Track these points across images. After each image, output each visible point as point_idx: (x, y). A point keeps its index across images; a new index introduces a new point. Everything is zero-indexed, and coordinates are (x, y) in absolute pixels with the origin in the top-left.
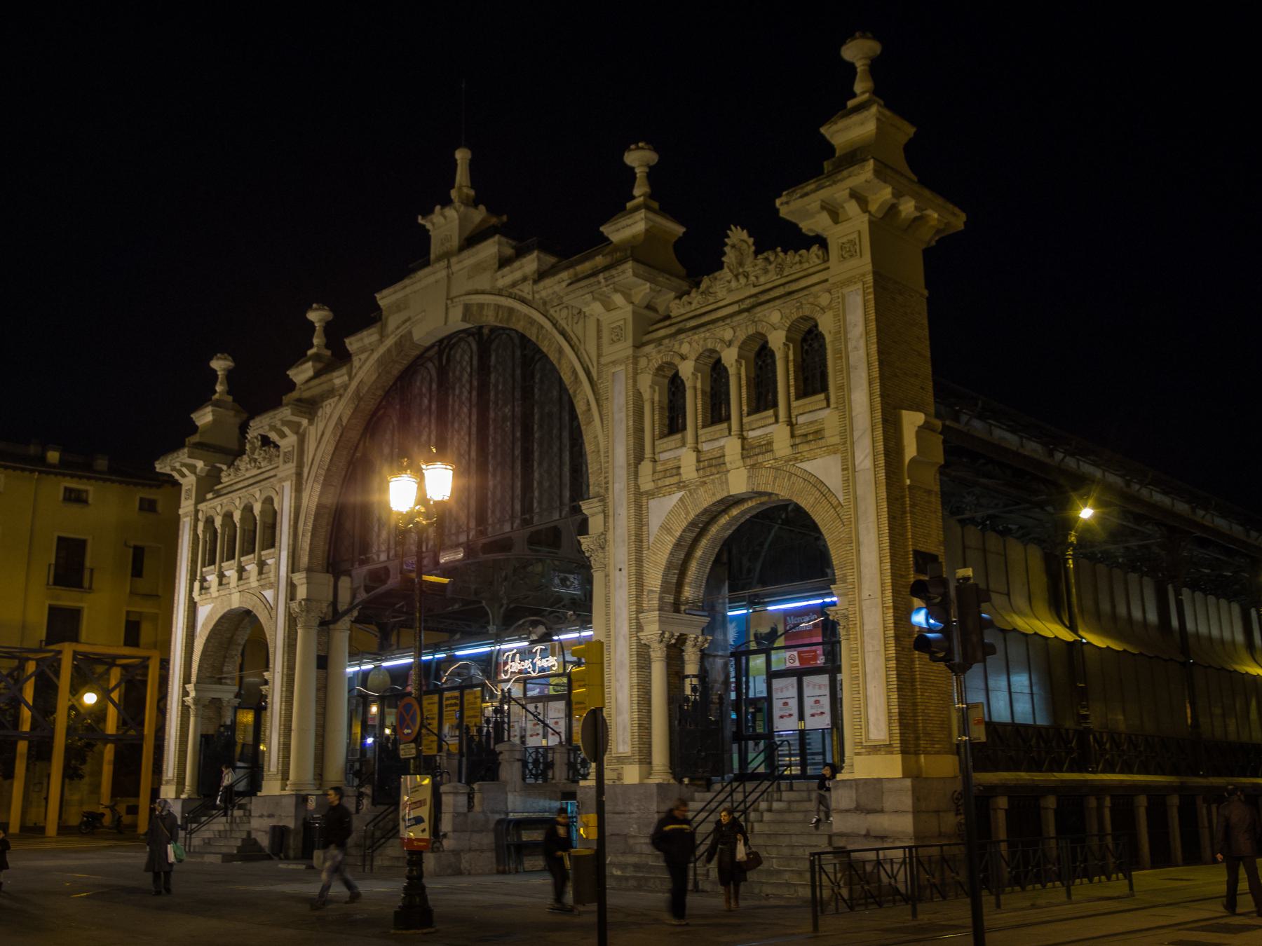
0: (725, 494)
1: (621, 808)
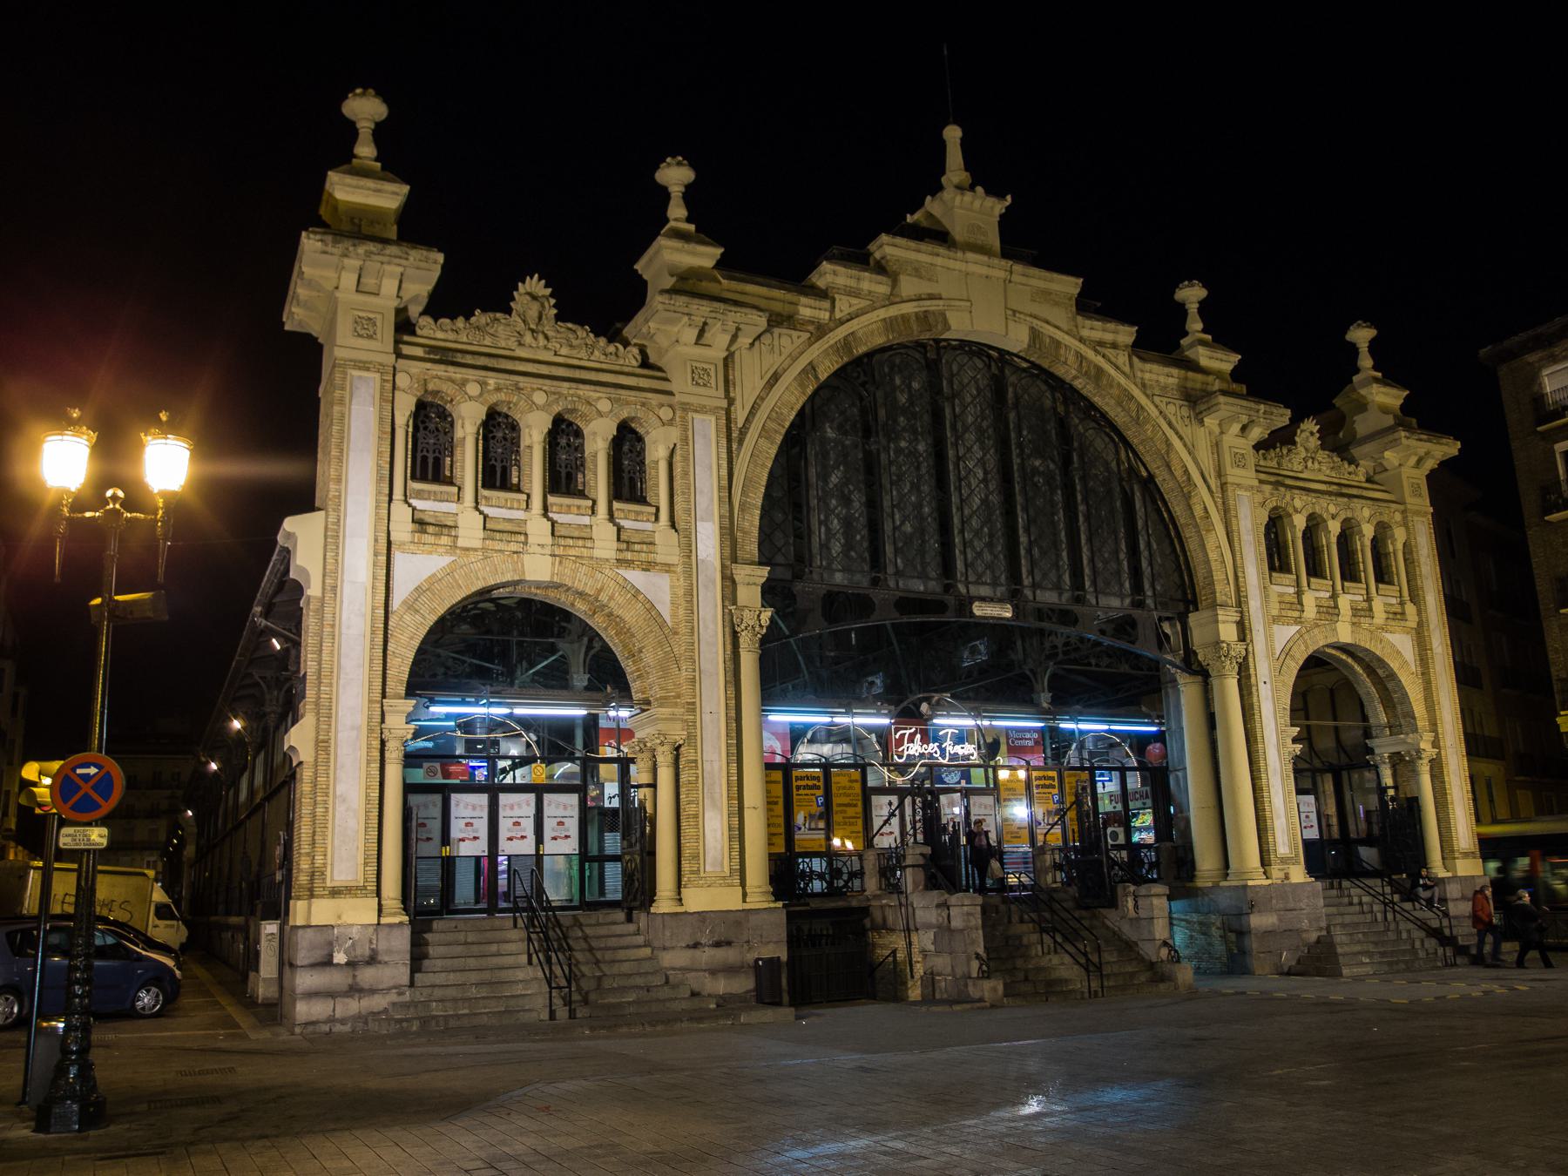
1: (1291, 905)
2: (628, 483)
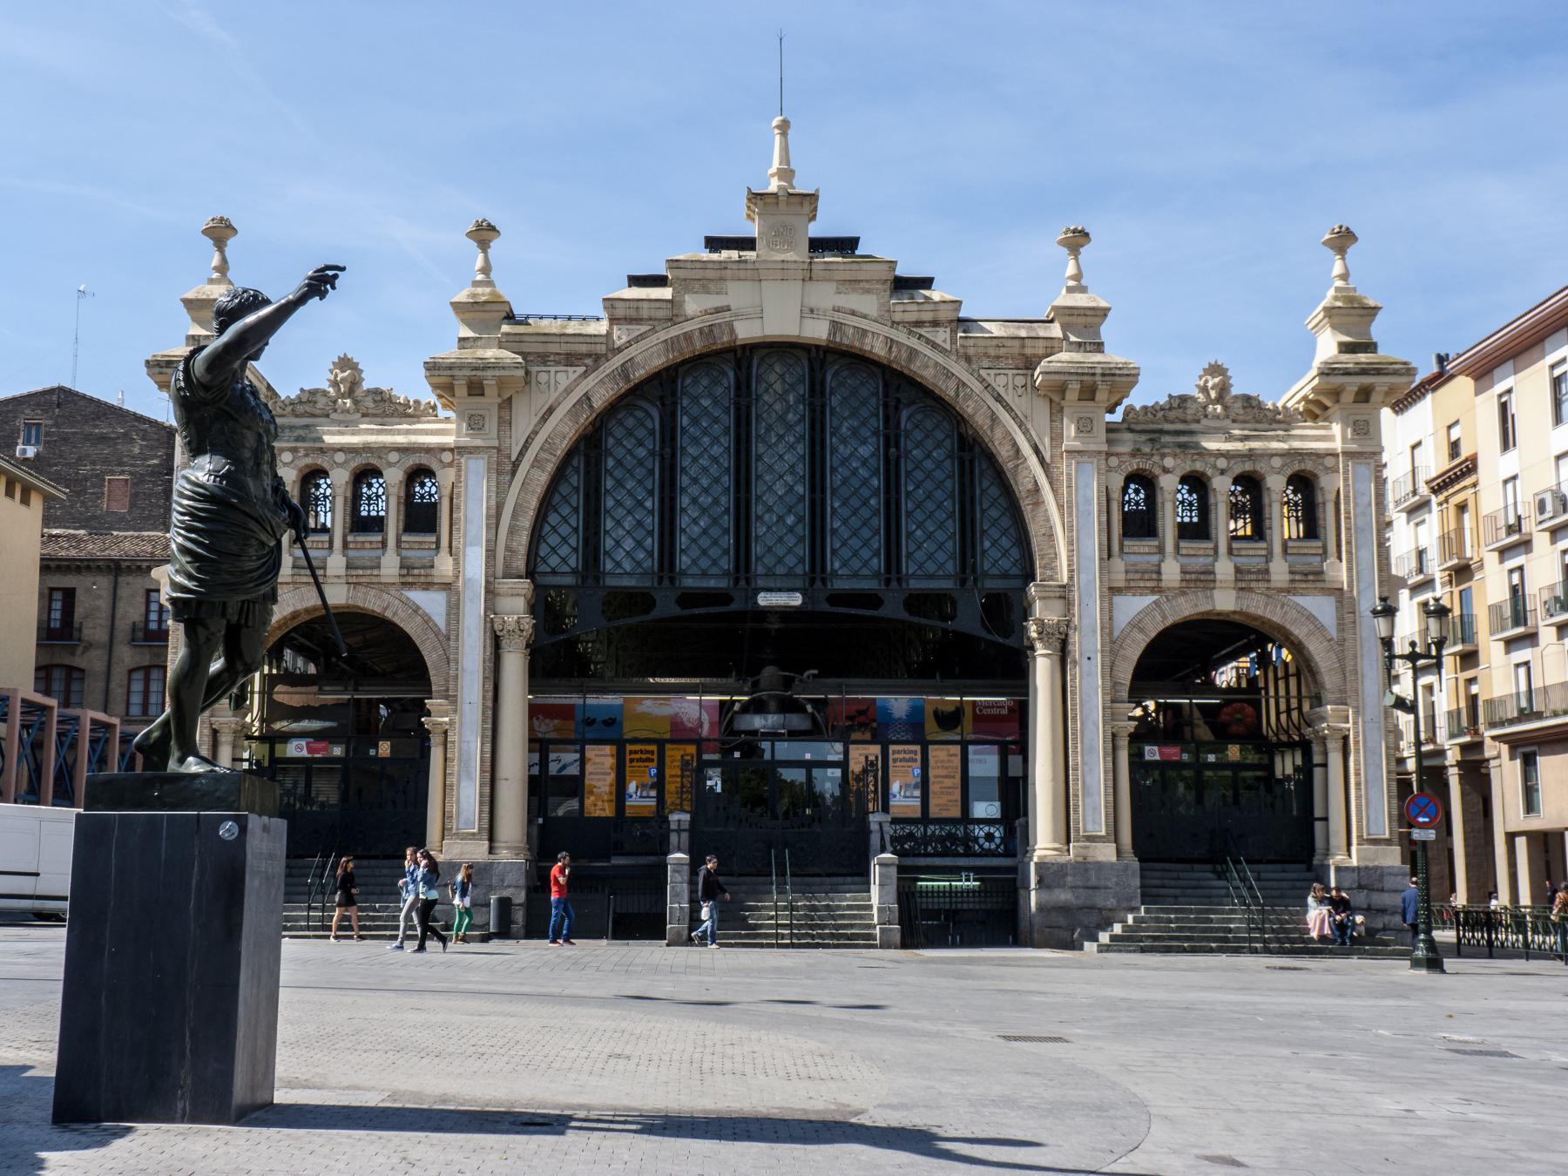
0: (1208, 608)
1: (1093, 881)
2: (421, 518)
